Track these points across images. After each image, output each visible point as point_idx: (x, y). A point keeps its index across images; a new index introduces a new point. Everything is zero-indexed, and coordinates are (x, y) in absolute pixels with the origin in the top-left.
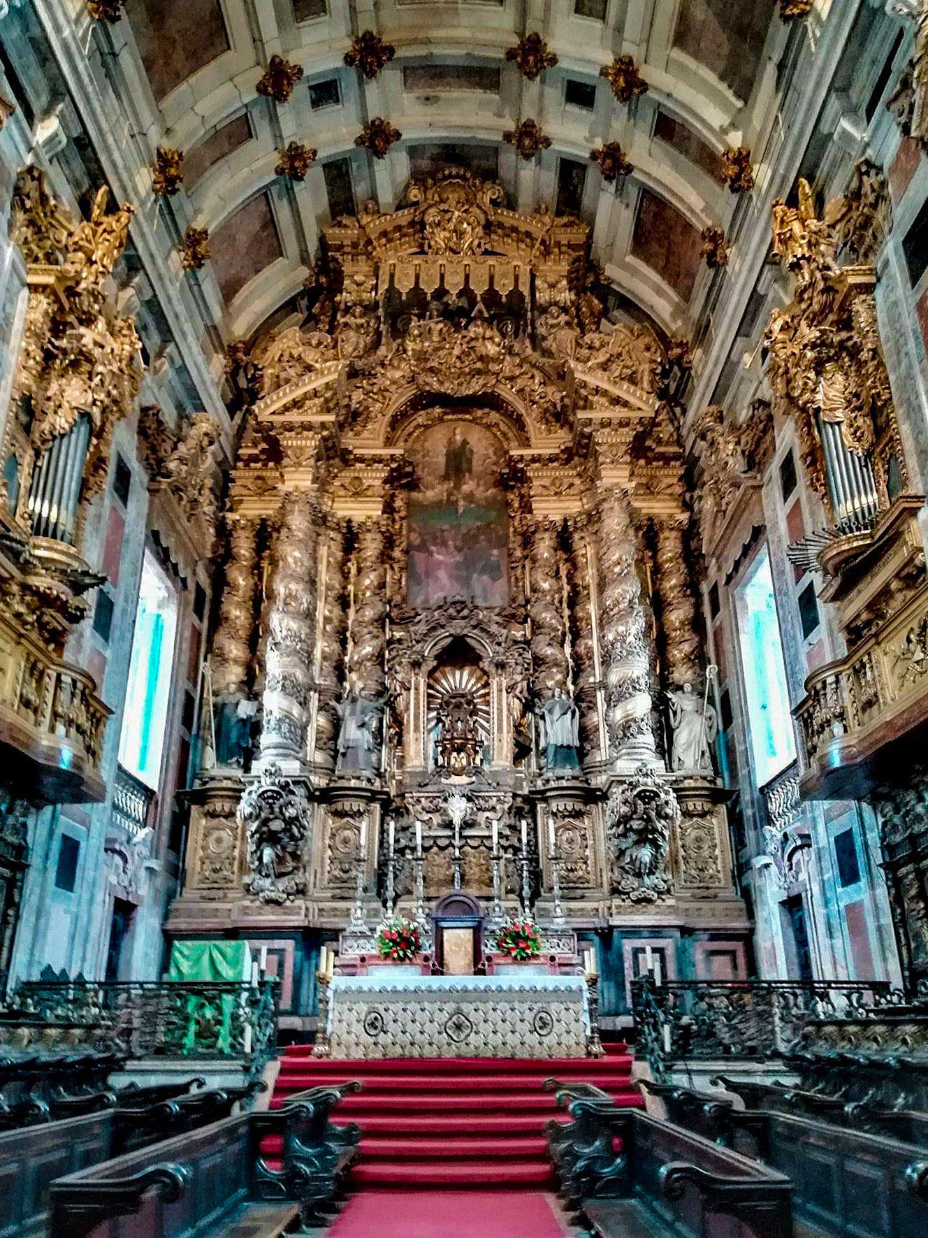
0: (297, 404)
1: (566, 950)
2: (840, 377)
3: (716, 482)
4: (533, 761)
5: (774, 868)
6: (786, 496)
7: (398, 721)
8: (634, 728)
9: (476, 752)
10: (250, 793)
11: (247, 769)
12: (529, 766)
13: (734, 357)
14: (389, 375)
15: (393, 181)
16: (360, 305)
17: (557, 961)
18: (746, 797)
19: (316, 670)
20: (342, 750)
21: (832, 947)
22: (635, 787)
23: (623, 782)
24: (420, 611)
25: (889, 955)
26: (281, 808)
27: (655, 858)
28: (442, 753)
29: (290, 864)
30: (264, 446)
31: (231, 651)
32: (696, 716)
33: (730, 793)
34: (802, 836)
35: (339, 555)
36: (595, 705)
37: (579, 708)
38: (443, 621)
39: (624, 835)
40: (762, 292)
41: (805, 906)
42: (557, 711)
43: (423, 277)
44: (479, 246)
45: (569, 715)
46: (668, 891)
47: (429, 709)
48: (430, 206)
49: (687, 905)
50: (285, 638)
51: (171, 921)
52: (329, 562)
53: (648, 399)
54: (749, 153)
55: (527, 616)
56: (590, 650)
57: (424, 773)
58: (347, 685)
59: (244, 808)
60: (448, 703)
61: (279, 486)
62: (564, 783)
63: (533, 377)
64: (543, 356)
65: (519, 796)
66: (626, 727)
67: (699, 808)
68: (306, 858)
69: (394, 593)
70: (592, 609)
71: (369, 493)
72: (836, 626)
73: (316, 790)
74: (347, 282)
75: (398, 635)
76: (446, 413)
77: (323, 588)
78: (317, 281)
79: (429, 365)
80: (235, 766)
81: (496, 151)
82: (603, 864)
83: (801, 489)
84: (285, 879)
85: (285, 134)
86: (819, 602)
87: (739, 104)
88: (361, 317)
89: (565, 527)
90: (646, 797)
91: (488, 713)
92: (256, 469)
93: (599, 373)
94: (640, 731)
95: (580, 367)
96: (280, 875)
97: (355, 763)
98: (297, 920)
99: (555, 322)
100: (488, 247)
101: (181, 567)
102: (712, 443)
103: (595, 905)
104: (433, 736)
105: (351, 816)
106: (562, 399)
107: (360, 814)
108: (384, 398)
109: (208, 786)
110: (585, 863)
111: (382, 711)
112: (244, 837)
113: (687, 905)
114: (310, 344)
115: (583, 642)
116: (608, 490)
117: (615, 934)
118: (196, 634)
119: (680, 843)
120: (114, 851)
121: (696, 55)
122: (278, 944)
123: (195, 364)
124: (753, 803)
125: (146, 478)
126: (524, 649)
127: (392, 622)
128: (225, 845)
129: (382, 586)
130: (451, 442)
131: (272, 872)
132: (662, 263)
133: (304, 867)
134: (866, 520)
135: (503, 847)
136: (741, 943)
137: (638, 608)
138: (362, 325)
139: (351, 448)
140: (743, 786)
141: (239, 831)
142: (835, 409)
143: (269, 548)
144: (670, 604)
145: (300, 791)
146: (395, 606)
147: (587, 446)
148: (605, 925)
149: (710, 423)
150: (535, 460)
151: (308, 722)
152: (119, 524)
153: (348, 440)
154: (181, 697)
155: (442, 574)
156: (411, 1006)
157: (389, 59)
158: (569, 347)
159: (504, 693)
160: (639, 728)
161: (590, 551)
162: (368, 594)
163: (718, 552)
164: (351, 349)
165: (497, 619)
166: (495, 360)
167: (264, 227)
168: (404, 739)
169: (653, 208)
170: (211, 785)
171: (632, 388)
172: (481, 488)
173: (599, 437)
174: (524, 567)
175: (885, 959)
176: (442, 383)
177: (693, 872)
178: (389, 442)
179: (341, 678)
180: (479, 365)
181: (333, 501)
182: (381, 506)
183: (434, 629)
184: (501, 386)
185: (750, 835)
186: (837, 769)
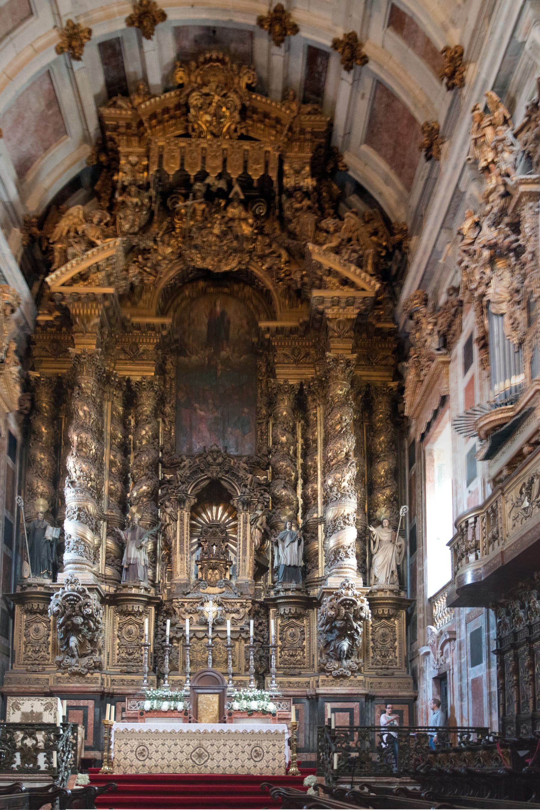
1: (285, 709)
4: (270, 577)
5: (432, 655)
7: (168, 546)
8: (342, 554)
9: (227, 569)
10: (57, 596)
11: (55, 579)
14: (160, 251)
15: (161, 58)
16: (135, 184)
18: (419, 605)
19: (104, 503)
20: (125, 566)
21: (461, 706)
22: (340, 596)
23: (330, 593)
24: (185, 458)
25: (493, 711)
26: (80, 607)
27: (351, 647)
29: (89, 648)
30: (57, 313)
31: (38, 487)
32: (390, 546)
33: (410, 601)
35: (120, 409)
36: (317, 535)
38: (202, 466)
39: (330, 631)
41: (448, 681)
42: (288, 540)
43: (188, 159)
45: (296, 543)
46: (359, 670)
47: (192, 537)
49: (372, 680)
52: (112, 415)
55: (269, 464)
56: (315, 491)
57: (187, 585)
58: (128, 516)
59: (53, 607)
60: (206, 532)
62: (290, 594)
63: (280, 256)
64: (289, 237)
65: (257, 602)
66: (337, 552)
67: (386, 613)
68: (101, 644)
70: (319, 458)
71: (145, 357)
73: (107, 595)
74: (123, 162)
75: (168, 477)
76: (208, 286)
77: (108, 437)
78: (98, 159)
79: (193, 243)
80: (46, 576)
81: (251, 35)
82: (315, 652)
84: (86, 658)
88: (135, 196)
89: (301, 390)
90: (346, 604)
91: (235, 539)
92: (51, 333)
93: (332, 255)
94: (347, 556)
95: (316, 248)
96: (82, 656)
97: (136, 575)
103: (307, 679)
104: (194, 557)
105: (133, 615)
106: (302, 277)
107: (141, 614)
108: (157, 272)
109: (27, 591)
110: (303, 650)
111: (156, 537)
113: (372, 680)
115: (310, 485)
116: (336, 360)
117: (320, 699)
118: (10, 473)
124: (424, 609)
129: (156, 436)
131: (76, 653)
132: (390, 152)
133: (100, 650)
135: (243, 638)
136: (407, 706)
137: (353, 459)
138: (137, 203)
139: (129, 316)
140: (419, 598)
141: (51, 623)
143: (65, 402)
144: (378, 457)
145: (94, 596)
146: (166, 453)
147: (321, 321)
148: (314, 693)
150: (279, 331)
151: (100, 545)
153: (126, 313)
155: (203, 427)
158: (310, 228)
159: (249, 525)
160: (346, 553)
161: (320, 412)
162: (144, 442)
163: (415, 416)
164: (127, 226)
165: (245, 465)
166: (247, 239)
168: (173, 558)
169: (385, 99)
170: (28, 590)
171: (358, 271)
173: (330, 313)
175: (491, 714)
176: (203, 259)
177: (378, 657)
178: (162, 312)
180: (235, 244)
181: (115, 364)
182: (154, 368)
183: (195, 473)
184: (253, 264)
185: (420, 632)
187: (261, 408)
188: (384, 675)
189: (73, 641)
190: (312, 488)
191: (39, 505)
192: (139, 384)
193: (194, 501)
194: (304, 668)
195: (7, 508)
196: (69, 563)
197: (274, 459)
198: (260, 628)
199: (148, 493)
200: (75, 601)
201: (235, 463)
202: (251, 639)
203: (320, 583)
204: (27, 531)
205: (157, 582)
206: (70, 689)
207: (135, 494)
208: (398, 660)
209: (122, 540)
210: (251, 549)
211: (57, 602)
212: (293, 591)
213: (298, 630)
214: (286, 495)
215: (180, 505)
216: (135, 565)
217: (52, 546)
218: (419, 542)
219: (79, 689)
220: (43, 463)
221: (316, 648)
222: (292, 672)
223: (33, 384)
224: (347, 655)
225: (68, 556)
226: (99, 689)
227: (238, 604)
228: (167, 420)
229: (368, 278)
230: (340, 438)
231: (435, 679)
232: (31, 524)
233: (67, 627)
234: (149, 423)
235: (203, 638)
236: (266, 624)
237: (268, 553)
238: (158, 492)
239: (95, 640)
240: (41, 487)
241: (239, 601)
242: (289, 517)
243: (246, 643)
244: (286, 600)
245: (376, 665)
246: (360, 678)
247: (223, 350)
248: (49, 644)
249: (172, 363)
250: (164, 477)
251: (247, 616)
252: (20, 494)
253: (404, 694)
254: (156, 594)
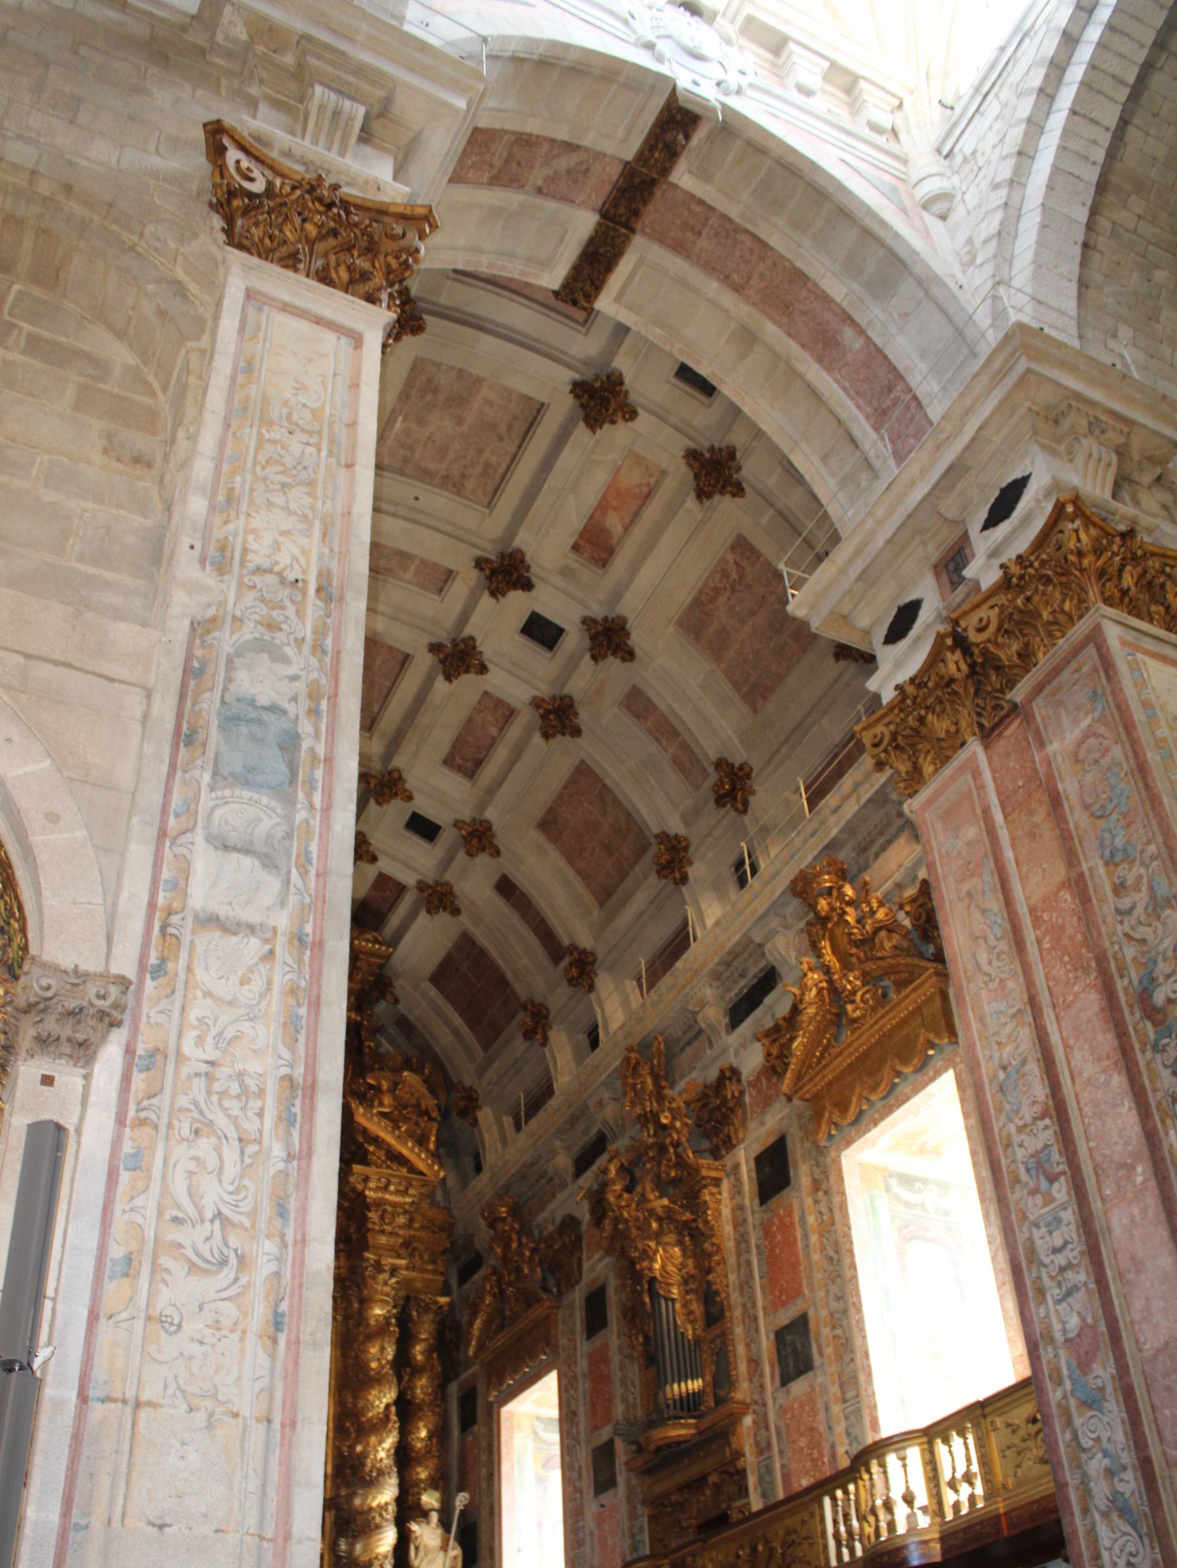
2: (677, 1251)
83: (613, 1336)
134: (690, 1404)
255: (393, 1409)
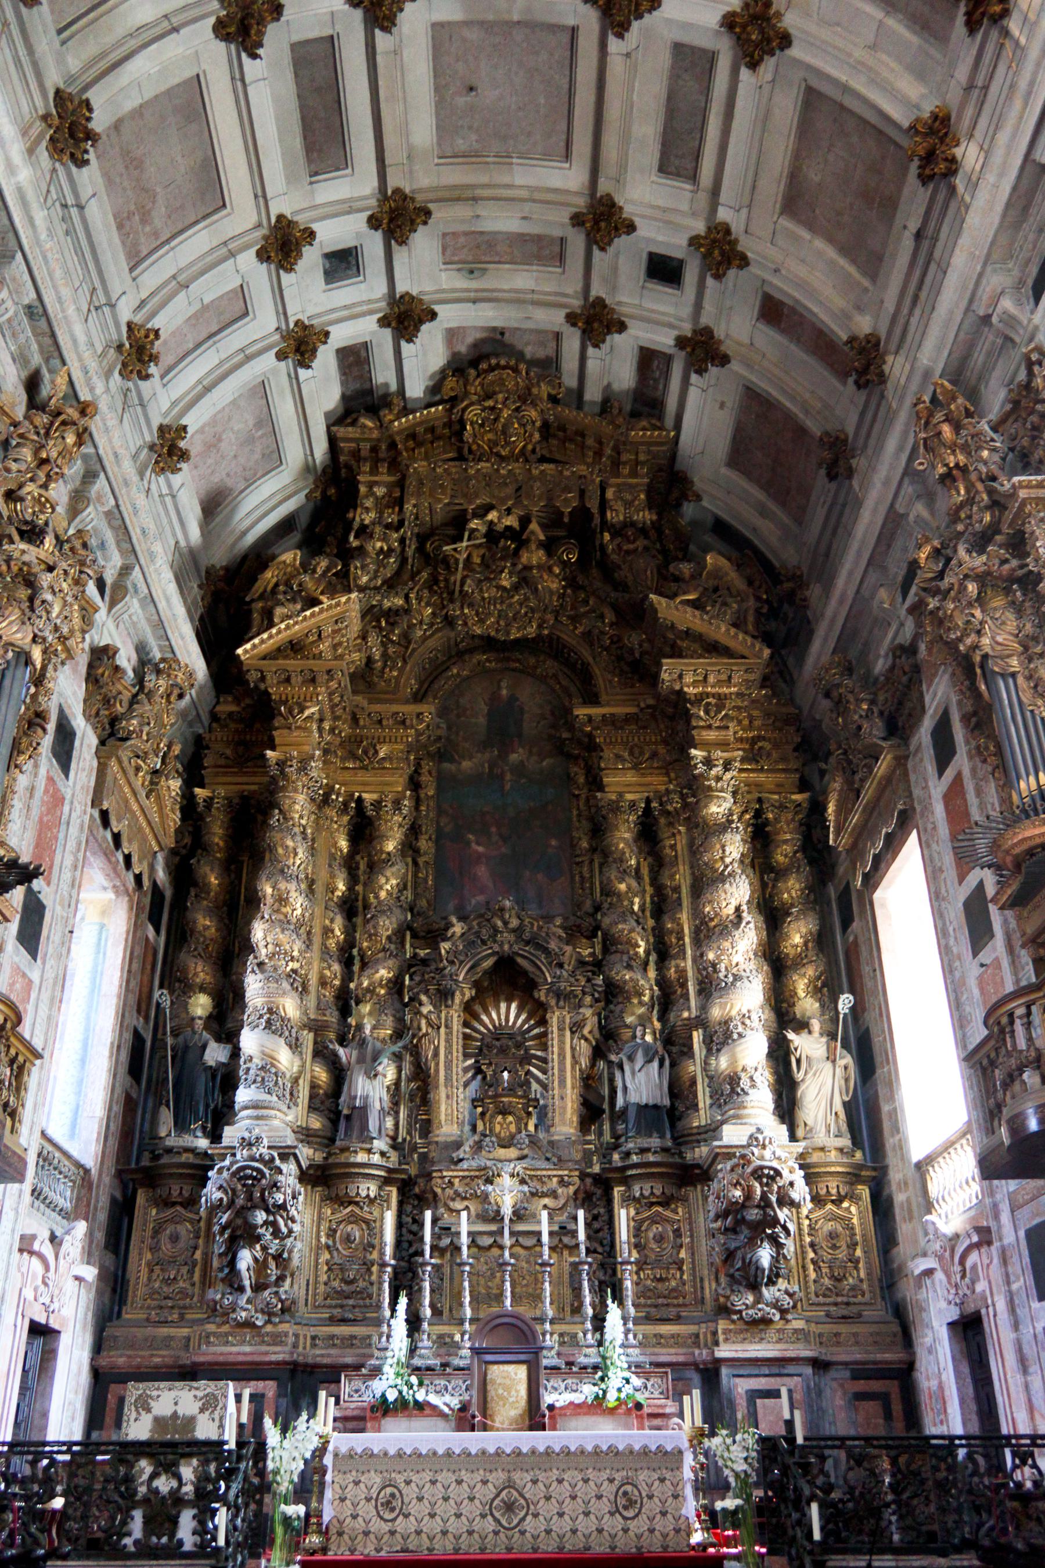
0: (294, 647)
1: (656, 1395)
2: (1010, 616)
3: (845, 753)
4: (606, 1127)
6: (941, 772)
8: (745, 1083)
9: (529, 1114)
10: (220, 1171)
11: (215, 1137)
12: (600, 1134)
13: (865, 592)
16: (379, 523)
17: (646, 1410)
18: (895, 1176)
20: (345, 1112)
21: (1027, 1387)
24: (454, 920)
27: (775, 1260)
28: (483, 1114)
30: (248, 701)
31: (196, 974)
34: (978, 1230)
35: (344, 844)
36: (691, 1047)
37: (670, 1054)
39: (733, 1230)
40: (902, 511)
44: (534, 451)
45: (656, 1064)
47: (466, 1056)
48: (472, 404)
50: (272, 956)
51: (104, 1353)
53: (753, 645)
54: (877, 344)
56: (682, 973)
57: (458, 1145)
59: (212, 1192)
61: (269, 753)
62: (651, 1158)
63: (602, 617)
64: (616, 590)
65: (589, 1175)
69: (416, 895)
70: (684, 917)
72: (1017, 943)
75: (422, 953)
78: (324, 492)
80: (199, 1134)
83: (962, 761)
85: (290, 312)
86: (993, 908)
87: (866, 283)
89: (648, 810)
97: (364, 1127)
98: (278, 1354)
99: (631, 547)
100: (545, 452)
101: (135, 859)
102: (839, 702)
103: (692, 1329)
105: (357, 1203)
109: (162, 1161)
110: (680, 1269)
112: (209, 1236)
114: (314, 571)
115: (673, 963)
117: (724, 1371)
118: (150, 950)
119: (808, 1239)
120: (31, 1253)
121: (811, 226)
122: (260, 1386)
123: (164, 592)
125: (93, 740)
126: (594, 973)
127: (412, 937)
128: (182, 1244)
130: (494, 697)
133: (292, 1275)
135: (566, 1246)
136: (896, 1382)
140: (892, 1160)
141: (202, 1224)
142: (1009, 656)
144: (789, 914)
149: (835, 676)
152: (56, 800)
154: (128, 1036)
155: (482, 871)
156: (443, 1477)
157: (425, 223)
159: (568, 1033)
161: (681, 842)
164: (365, 579)
167: (259, 424)
168: (431, 1096)
170: (165, 1160)
172: (535, 758)
174: (592, 861)
178: (418, 697)
179: (345, 1011)
186: (1035, 1133)
187: (580, 839)
188: (844, 1317)
189: (245, 1259)
190: (677, 966)
191: (197, 1005)
192: (378, 805)
193: (468, 994)
194: (685, 1305)
195: (139, 1011)
196: (246, 1108)
197: (606, 921)
198: (596, 1225)
199: (389, 980)
200: (254, 1178)
201: (540, 928)
202: (583, 1248)
203: (703, 1136)
204: (172, 1050)
205: (400, 1140)
206: (231, 1359)
207: (365, 984)
208: (865, 1286)
209: (340, 1063)
210: (573, 1077)
211: (220, 1182)
212: (655, 1152)
213: (669, 1228)
214: (632, 979)
215: (446, 1000)
216: (364, 1110)
217: (214, 1077)
218: (878, 1059)
219: (249, 1359)
220: (207, 934)
221: (705, 1263)
222: (664, 1313)
223: (201, 808)
224: (769, 1277)
225: (243, 1095)
226: (287, 1358)
227: (555, 1180)
228: (421, 861)
229: (749, 640)
230: (723, 882)
231: (951, 1325)
232: (181, 1039)
233: (233, 1231)
234: (393, 865)
235: (491, 1246)
236: (606, 1218)
237: (602, 1084)
238: (404, 981)
239: (285, 1255)
240: (201, 971)
241: (555, 1173)
242: (640, 1017)
243: (571, 1255)
244: (639, 1171)
245: (824, 1296)
246: (799, 1324)
247: (513, 752)
248: (194, 1265)
249: (430, 773)
250: (415, 955)
251: (571, 1203)
252: (161, 987)
253: (888, 1356)
254: (400, 1164)
255: (745, 907)
